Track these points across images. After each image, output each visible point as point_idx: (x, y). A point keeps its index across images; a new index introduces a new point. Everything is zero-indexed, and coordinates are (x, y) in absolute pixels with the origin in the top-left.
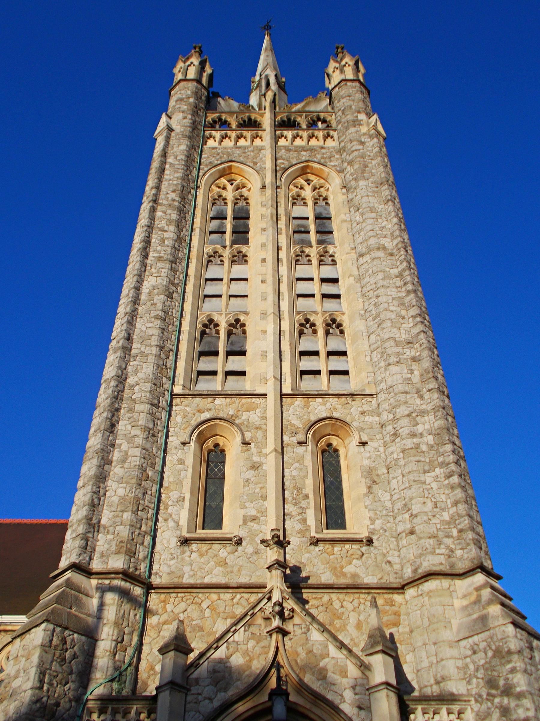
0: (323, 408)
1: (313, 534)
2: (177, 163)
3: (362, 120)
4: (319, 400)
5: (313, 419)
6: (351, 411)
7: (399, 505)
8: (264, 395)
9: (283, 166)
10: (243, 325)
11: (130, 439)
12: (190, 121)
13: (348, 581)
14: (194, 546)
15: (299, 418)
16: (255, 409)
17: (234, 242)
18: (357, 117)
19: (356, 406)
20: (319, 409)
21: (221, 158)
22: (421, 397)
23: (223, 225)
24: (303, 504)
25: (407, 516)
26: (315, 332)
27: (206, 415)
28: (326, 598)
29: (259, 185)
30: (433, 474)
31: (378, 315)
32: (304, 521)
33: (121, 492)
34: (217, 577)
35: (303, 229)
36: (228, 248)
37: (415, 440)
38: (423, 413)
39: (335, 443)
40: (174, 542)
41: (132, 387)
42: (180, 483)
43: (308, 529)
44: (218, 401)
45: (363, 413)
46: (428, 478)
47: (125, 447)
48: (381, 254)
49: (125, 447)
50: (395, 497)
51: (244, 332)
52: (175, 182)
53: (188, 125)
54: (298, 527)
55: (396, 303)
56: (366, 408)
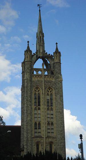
6: (53, 140)
8: (43, 138)
10: (40, 123)
17: (38, 106)
19: (54, 140)
20: (50, 140)
23: (36, 101)
26: (50, 125)
27: (37, 141)
29: (42, 93)
31: (58, 125)
38: (62, 142)
47: (29, 147)
48: (59, 113)
51: (40, 124)
56: (55, 140)
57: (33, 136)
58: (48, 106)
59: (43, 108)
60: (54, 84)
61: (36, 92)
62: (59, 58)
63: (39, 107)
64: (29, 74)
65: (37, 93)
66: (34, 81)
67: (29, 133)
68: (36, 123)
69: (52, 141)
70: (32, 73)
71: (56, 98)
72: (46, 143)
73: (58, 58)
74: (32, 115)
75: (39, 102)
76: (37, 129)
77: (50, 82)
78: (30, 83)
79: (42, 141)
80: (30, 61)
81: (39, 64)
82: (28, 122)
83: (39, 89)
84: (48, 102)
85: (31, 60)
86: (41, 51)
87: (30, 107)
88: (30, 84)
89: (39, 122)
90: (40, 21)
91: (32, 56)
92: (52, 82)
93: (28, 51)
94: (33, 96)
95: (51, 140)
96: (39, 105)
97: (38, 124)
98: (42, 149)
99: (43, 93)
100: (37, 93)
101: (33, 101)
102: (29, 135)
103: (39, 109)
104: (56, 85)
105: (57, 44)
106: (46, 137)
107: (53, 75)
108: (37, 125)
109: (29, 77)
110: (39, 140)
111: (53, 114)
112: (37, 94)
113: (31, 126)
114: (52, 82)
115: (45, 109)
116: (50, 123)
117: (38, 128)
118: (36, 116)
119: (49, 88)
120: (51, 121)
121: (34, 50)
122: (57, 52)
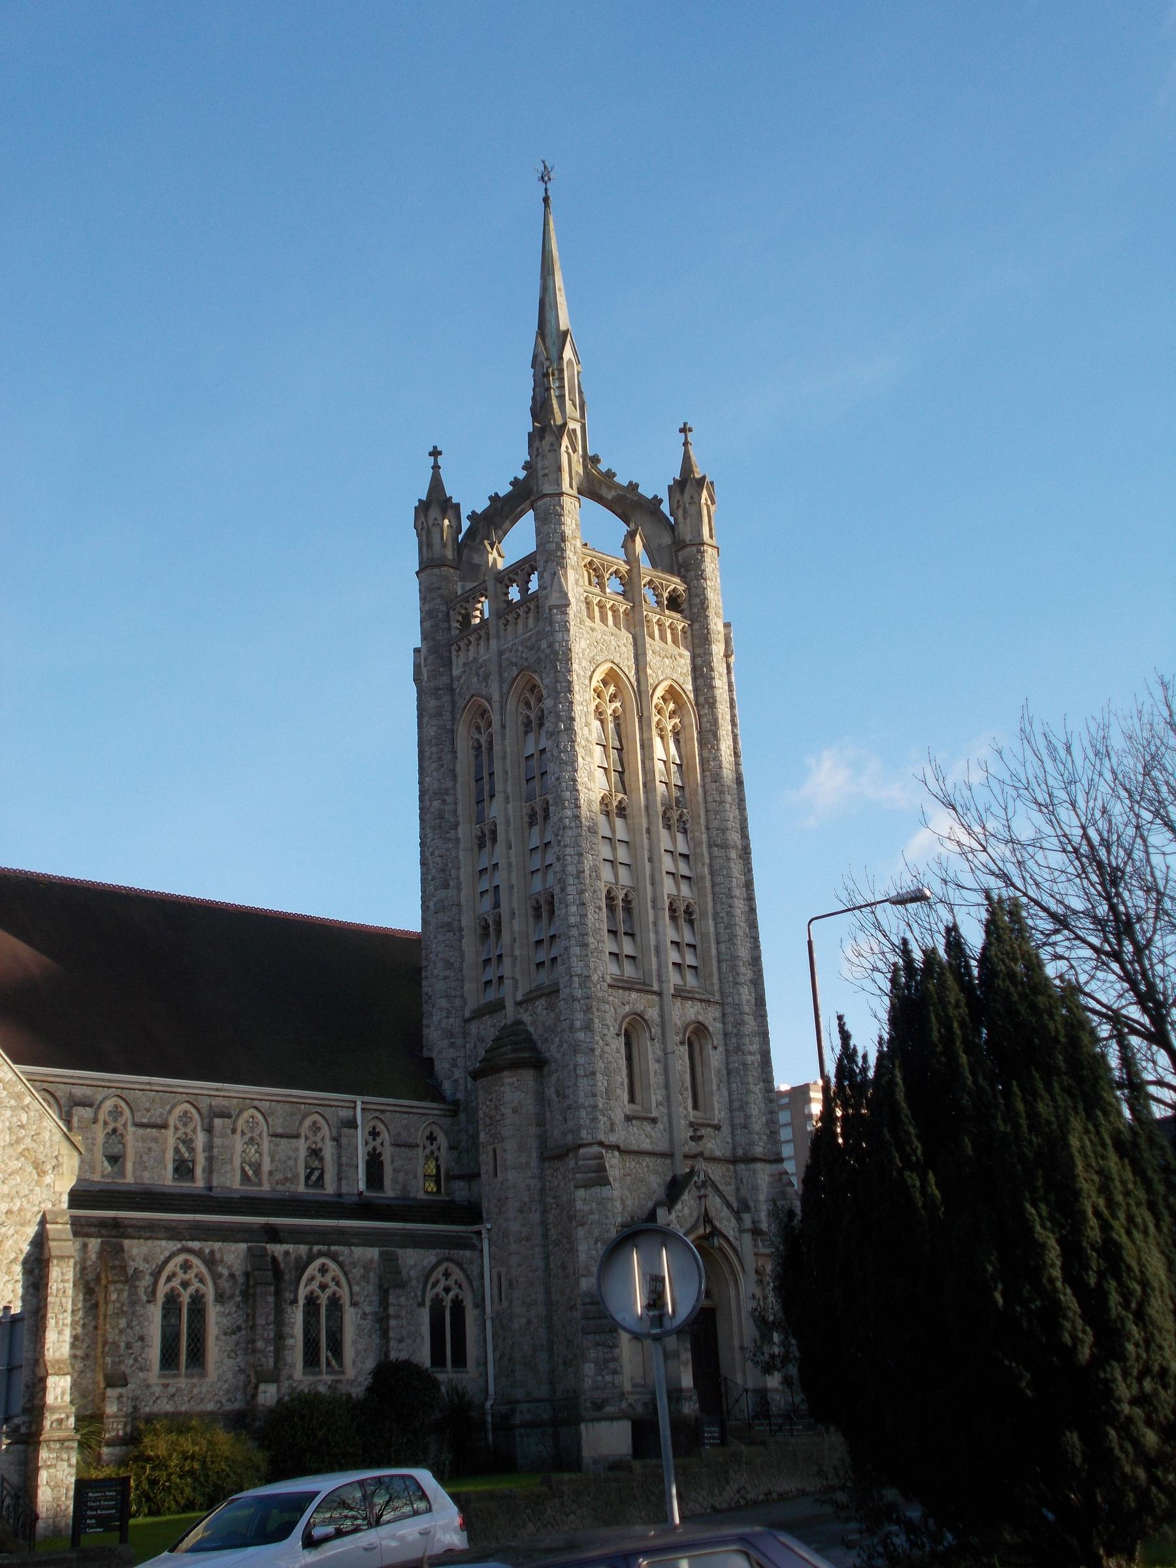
5: (688, 1020)
7: (736, 1104)
34: (646, 1145)
43: (688, 1114)
44: (634, 995)
50: (734, 1097)
69: (701, 1019)
79: (652, 1014)
122: (688, 484)
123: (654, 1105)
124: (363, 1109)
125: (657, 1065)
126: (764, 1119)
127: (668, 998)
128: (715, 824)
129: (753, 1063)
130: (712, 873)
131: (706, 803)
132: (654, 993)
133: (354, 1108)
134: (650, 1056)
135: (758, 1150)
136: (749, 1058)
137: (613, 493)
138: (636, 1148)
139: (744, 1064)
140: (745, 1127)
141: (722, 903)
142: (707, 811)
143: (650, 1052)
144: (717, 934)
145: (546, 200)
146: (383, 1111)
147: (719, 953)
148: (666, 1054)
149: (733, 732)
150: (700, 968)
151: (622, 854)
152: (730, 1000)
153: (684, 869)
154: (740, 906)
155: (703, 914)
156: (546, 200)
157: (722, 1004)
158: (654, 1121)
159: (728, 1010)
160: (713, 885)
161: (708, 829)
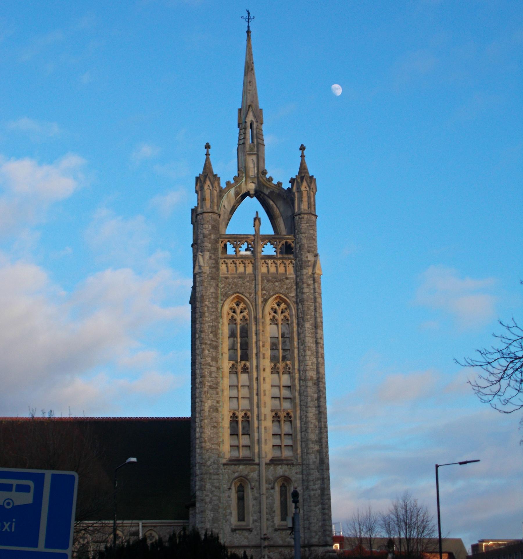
0: (281, 470)
1: (276, 527)
2: (210, 305)
3: (309, 261)
4: (280, 466)
5: (278, 475)
7: (306, 517)
8: (259, 464)
9: (265, 297)
10: (248, 417)
11: (212, 492)
12: (214, 261)
13: (286, 544)
14: (237, 532)
15: (272, 475)
16: (255, 471)
17: (242, 359)
18: (307, 257)
20: (280, 470)
21: (232, 288)
22: (318, 471)
24: (273, 514)
25: (308, 522)
28: (280, 550)
30: (318, 507)
32: (273, 522)
33: (212, 515)
35: (274, 347)
36: (239, 364)
37: (314, 492)
39: (286, 484)
40: (230, 529)
41: (209, 467)
42: (229, 506)
43: (274, 525)
44: (241, 467)
45: (296, 473)
46: (316, 509)
47: (211, 496)
49: (211, 496)
50: (305, 513)
52: (211, 324)
53: (213, 265)
54: (272, 524)
55: (314, 417)
56: (298, 470)
57: (224, 461)
58: (274, 359)
59: (257, 367)
60: (291, 288)
61: (234, 312)
62: (309, 197)
63: (245, 365)
64: (210, 258)
65: (239, 317)
66: (227, 278)
67: (211, 449)
68: (234, 419)
69: (286, 474)
70: (220, 250)
71: (299, 334)
72: (268, 481)
73: (305, 199)
74: (223, 391)
75: (245, 347)
76: (237, 435)
77: (281, 280)
78: (214, 285)
79: (254, 475)
80: (214, 213)
81: (247, 218)
82: (207, 414)
83: (245, 302)
84: (274, 347)
85: (218, 206)
86: (253, 172)
87: (213, 363)
88: (212, 290)
89: (245, 414)
90: (249, 68)
91: (221, 193)
92: (287, 278)
93: (206, 178)
94: (225, 329)
95: (285, 471)
96: (245, 357)
97: (240, 419)
98: (255, 499)
99: (256, 318)
100: (239, 317)
101: (225, 344)
102: (209, 458)
103: (245, 370)
104: (299, 290)
105: (302, 148)
106: (268, 461)
107: (291, 256)
108: (240, 423)
109: (211, 267)
110: (246, 473)
111: (289, 387)
112: (238, 321)
113: (216, 426)
114: (287, 278)
115: (264, 370)
116: (282, 415)
117: (240, 432)
118: (234, 393)
119: (276, 298)
120: (284, 410)
121: (226, 169)
123: (251, 522)
124: (143, 526)
125: (255, 502)
126: (320, 524)
127: (263, 466)
128: (302, 368)
129: (314, 495)
130: (300, 394)
131: (299, 357)
132: (256, 464)
133: (139, 526)
134: (251, 497)
135: (315, 540)
136: (312, 493)
137: (269, 191)
138: (237, 545)
139: (309, 496)
140: (309, 529)
141: (303, 411)
142: (299, 361)
143: (250, 495)
144: (301, 427)
145: (248, 32)
146: (155, 526)
147: (302, 438)
148: (260, 495)
149: (315, 315)
150: (294, 446)
151: (244, 392)
152: (305, 462)
153: (285, 393)
154: (312, 412)
155: (295, 417)
156: (248, 32)
157: (302, 465)
158: (250, 530)
159: (304, 467)
160: (300, 401)
161: (299, 371)
